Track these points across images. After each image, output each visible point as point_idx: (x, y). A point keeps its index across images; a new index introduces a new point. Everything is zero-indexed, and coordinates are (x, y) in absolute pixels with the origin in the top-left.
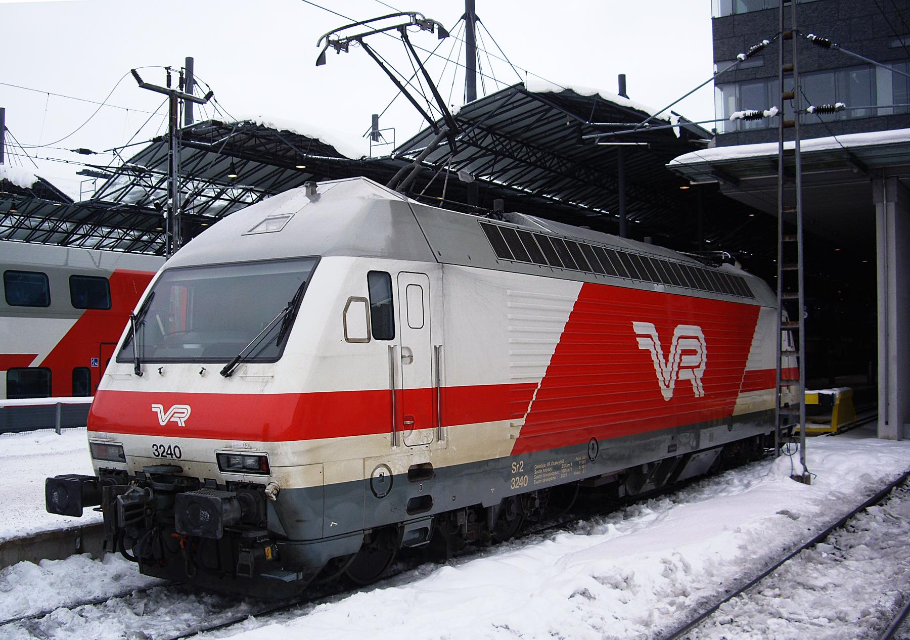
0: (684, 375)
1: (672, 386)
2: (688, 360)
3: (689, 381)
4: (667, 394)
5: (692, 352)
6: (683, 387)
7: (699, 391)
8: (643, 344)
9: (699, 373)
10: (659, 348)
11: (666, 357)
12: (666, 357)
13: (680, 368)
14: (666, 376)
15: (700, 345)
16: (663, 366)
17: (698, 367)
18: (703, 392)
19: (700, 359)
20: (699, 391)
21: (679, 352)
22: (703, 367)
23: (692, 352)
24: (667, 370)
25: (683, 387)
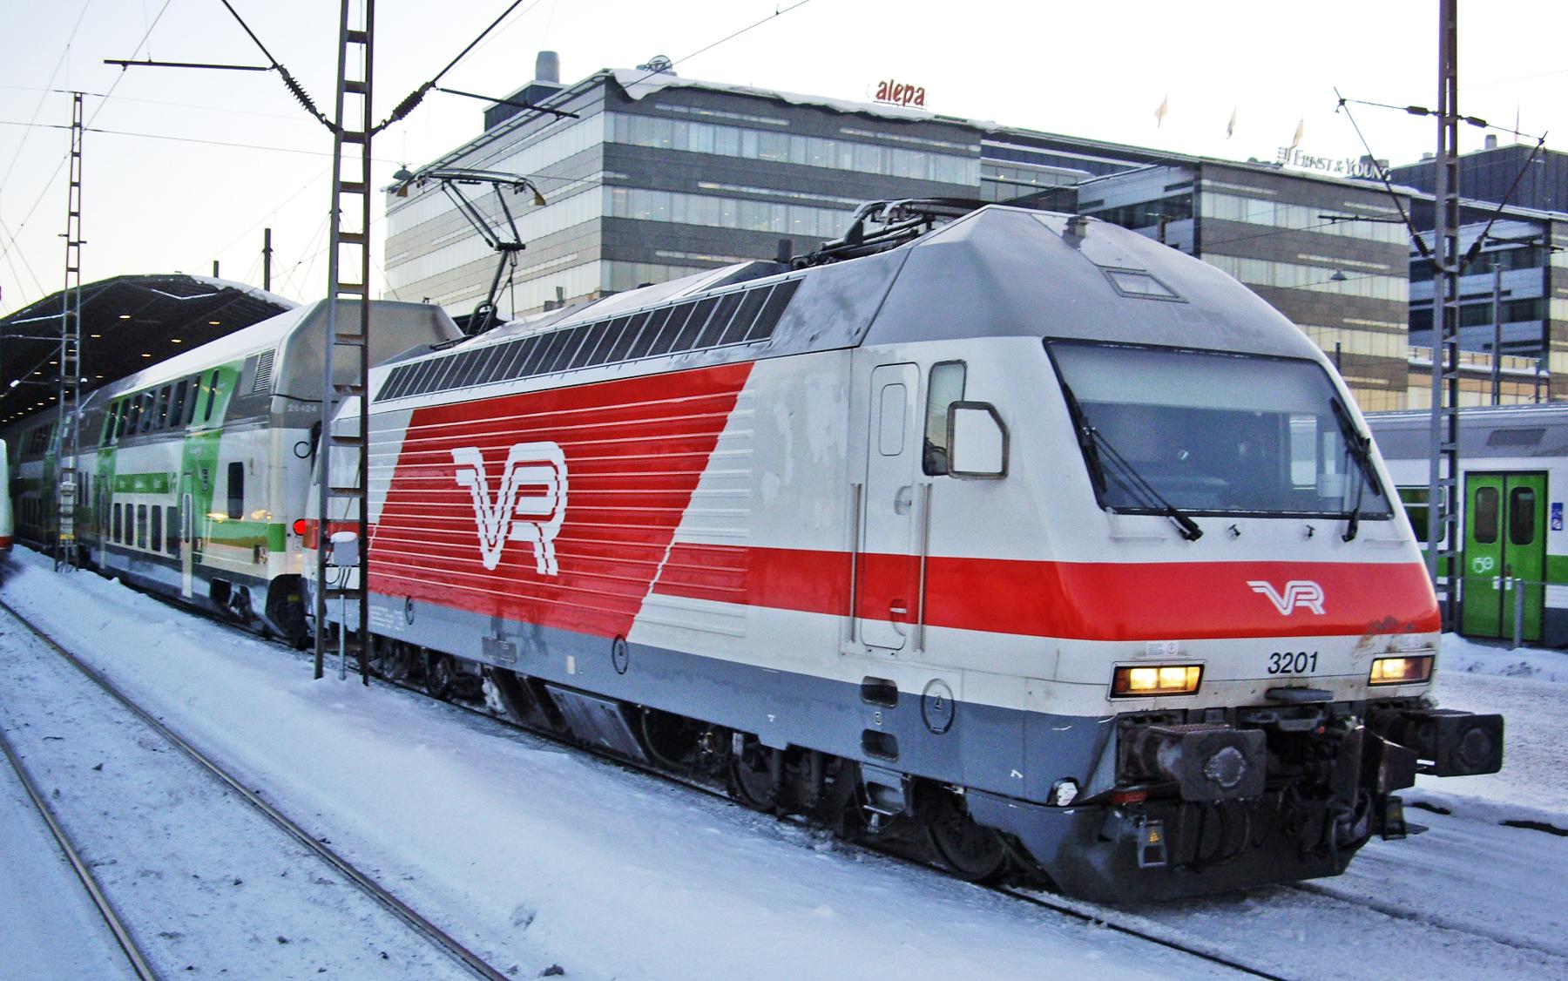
0: (523, 532)
1: (500, 546)
2: (528, 505)
3: (529, 545)
4: (491, 560)
5: (539, 490)
6: (517, 553)
7: (548, 564)
8: (463, 478)
9: (552, 529)
10: (485, 486)
11: (494, 499)
12: (494, 499)
13: (515, 516)
14: (491, 528)
15: (557, 481)
16: (488, 513)
17: (549, 518)
18: (554, 570)
19: (556, 502)
20: (548, 564)
21: (515, 489)
22: (559, 518)
23: (539, 490)
24: (492, 521)
25: (517, 553)
